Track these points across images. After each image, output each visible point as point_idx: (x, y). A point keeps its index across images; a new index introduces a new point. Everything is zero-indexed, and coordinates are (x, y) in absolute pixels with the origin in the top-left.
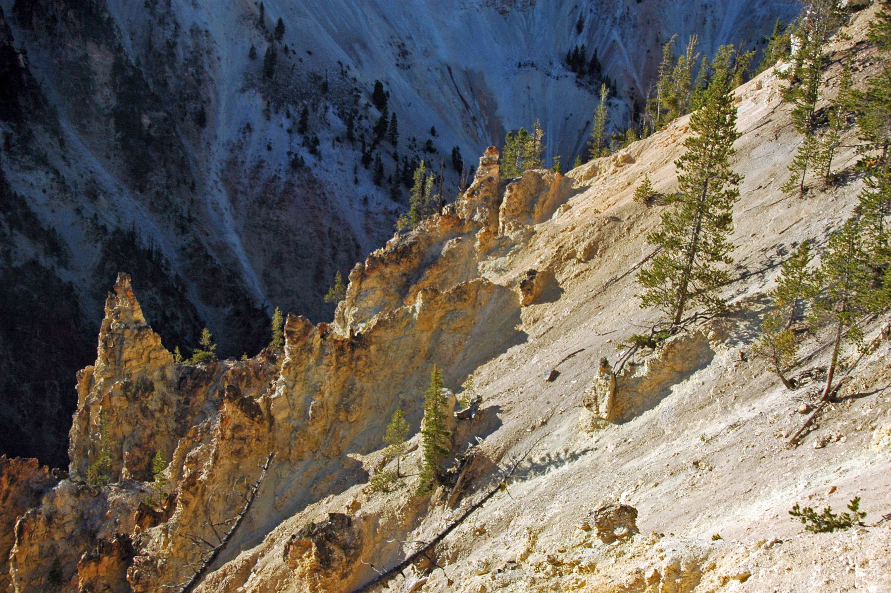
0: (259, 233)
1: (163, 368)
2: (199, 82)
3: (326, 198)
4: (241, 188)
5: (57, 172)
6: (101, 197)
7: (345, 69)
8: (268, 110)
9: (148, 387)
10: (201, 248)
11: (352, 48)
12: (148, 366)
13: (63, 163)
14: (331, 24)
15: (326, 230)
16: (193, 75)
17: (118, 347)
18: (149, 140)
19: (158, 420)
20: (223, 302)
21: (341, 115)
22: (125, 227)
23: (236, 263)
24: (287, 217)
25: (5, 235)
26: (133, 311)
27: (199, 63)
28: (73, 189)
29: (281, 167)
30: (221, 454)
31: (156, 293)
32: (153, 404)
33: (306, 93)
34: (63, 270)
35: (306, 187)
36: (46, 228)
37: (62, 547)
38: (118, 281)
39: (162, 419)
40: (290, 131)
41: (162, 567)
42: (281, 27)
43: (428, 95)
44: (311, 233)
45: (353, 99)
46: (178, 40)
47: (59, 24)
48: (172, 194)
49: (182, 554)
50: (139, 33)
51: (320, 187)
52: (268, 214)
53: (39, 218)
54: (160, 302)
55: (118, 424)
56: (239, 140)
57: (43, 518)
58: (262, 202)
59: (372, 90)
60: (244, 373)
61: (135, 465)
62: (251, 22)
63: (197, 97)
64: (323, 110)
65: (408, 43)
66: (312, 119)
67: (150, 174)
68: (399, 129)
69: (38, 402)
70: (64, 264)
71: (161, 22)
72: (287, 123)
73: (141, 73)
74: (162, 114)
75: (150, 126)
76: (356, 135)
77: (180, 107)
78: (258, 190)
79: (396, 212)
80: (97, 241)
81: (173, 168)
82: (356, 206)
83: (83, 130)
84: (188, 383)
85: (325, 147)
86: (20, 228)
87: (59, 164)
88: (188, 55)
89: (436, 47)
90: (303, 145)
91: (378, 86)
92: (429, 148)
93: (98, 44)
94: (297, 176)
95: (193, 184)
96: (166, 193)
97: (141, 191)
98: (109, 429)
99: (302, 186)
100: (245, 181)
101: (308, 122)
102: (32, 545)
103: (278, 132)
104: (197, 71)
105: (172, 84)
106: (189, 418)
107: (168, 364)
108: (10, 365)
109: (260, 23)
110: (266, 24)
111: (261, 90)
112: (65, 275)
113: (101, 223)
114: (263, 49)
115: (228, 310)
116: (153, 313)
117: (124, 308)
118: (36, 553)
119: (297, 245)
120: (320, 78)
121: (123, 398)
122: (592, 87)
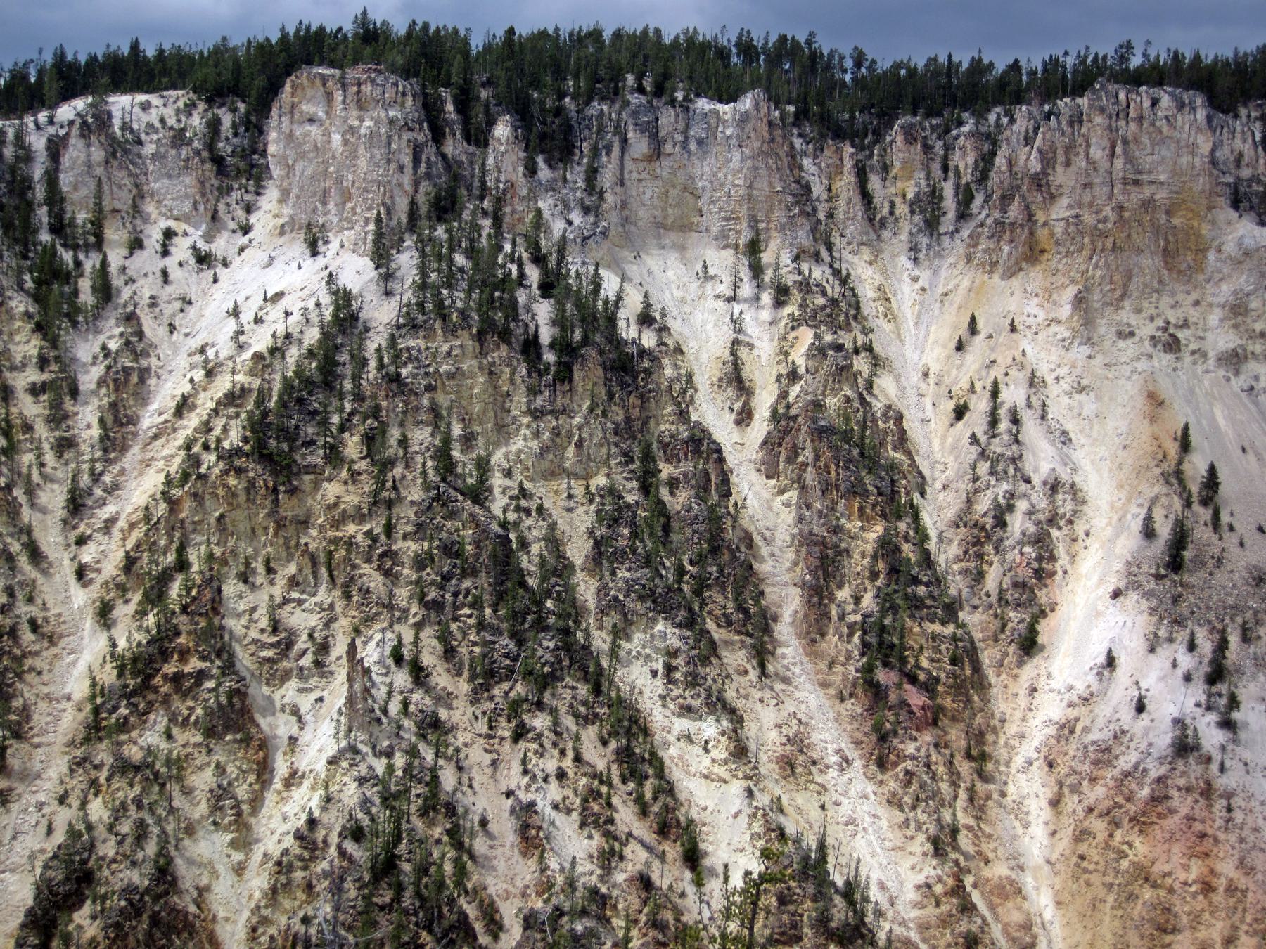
15: (1221, 884)
42: (1212, 482)
99: (1188, 790)
104: (1040, 559)
109: (1176, 476)
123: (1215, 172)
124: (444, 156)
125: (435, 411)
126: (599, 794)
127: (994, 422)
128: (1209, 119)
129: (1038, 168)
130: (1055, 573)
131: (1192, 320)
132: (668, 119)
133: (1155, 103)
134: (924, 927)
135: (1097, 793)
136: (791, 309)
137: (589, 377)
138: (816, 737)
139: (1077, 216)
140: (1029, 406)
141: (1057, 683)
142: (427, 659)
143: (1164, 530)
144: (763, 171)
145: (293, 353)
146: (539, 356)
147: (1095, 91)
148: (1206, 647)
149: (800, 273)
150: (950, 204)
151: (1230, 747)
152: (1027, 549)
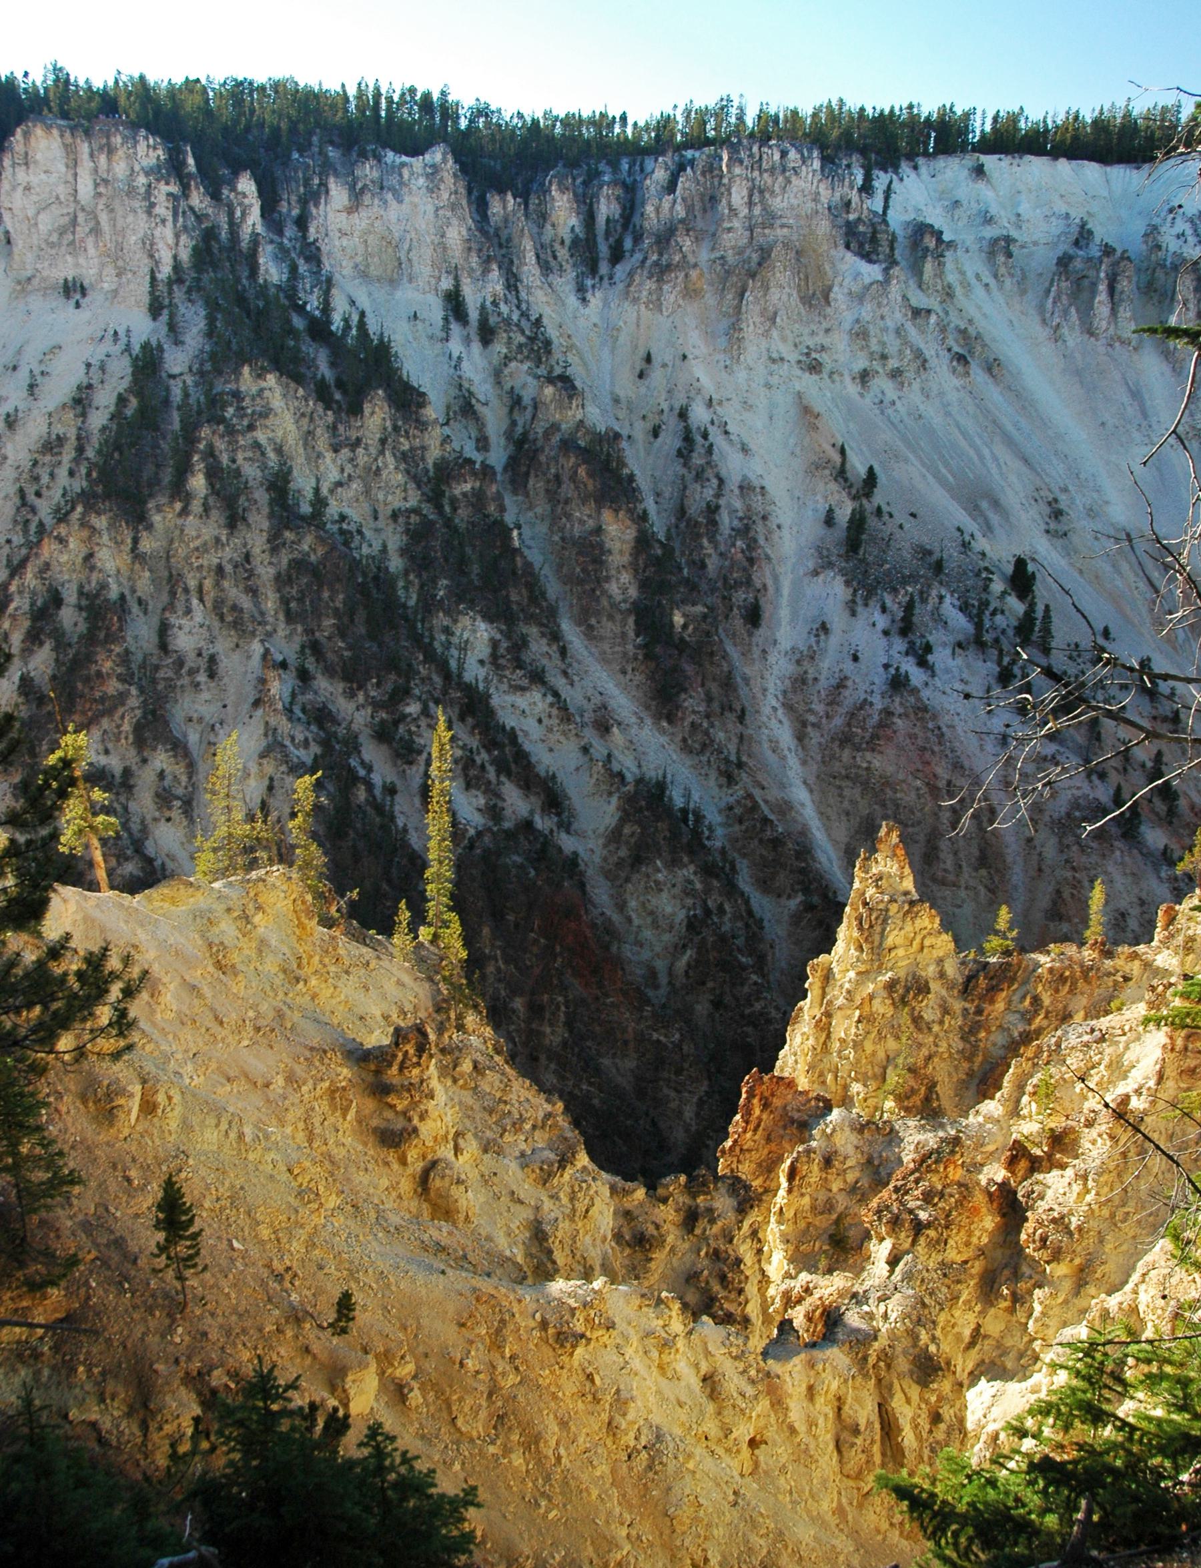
0: (840, 787)
1: (940, 961)
2: (751, 561)
3: (943, 735)
4: (812, 719)
5: (556, 694)
6: (615, 730)
7: (967, 538)
8: (853, 601)
9: (923, 989)
10: (755, 807)
11: (977, 507)
12: (920, 957)
13: (564, 681)
14: (944, 471)
15: (942, 784)
16: (743, 551)
17: (878, 929)
18: (681, 646)
19: (937, 1036)
20: (788, 891)
21: (964, 608)
22: (652, 773)
23: (804, 832)
24: (881, 763)
25: (489, 782)
26: (901, 878)
27: (752, 534)
28: (578, 719)
29: (875, 688)
30: (1168, 1072)
31: (695, 873)
32: (929, 1009)
33: (910, 576)
34: (563, 835)
35: (912, 716)
36: (543, 774)
37: (842, 1202)
38: (883, 832)
39: (942, 1034)
40: (886, 633)
41: (1080, 1229)
42: (871, 479)
43: (1097, 577)
44: (918, 789)
45: (981, 583)
46: (722, 502)
47: (564, 486)
48: (713, 726)
49: (1106, 1212)
50: (667, 495)
51: (934, 717)
53: (533, 759)
54: (698, 886)
55: (881, 1038)
56: (810, 647)
57: (818, 1158)
58: (845, 739)
59: (1009, 569)
60: (1067, 973)
61: (908, 1098)
62: (827, 472)
63: (749, 582)
65: (1062, 497)
66: (921, 614)
67: (683, 696)
68: (1053, 628)
69: (534, 1026)
70: (566, 826)
71: (699, 476)
72: (882, 622)
73: (673, 549)
74: (700, 609)
75: (685, 626)
76: (987, 638)
77: (724, 598)
78: (838, 721)
79: (1053, 757)
80: (610, 794)
81: (714, 688)
82: (990, 748)
83: (590, 633)
84: (980, 983)
85: (940, 657)
86: (509, 775)
87: (560, 683)
88: (736, 523)
89: (1107, 503)
90: (907, 654)
91: (1020, 563)
93: (616, 511)
94: (898, 700)
95: (743, 711)
96: (705, 725)
97: (670, 722)
98: (869, 1047)
99: (907, 716)
100: (819, 708)
101: (915, 619)
102: (802, 1195)
103: (867, 638)
104: (748, 546)
105: (712, 564)
106: (983, 1034)
107: (947, 955)
108: (499, 970)
109: (841, 474)
110: (849, 475)
112: (568, 843)
113: (616, 767)
114: (844, 512)
115: (794, 903)
116: (689, 902)
117: (886, 871)
118: (807, 1207)
119: (897, 806)
120: (930, 553)
121: (888, 1002)
124: (191, 208)
125: (257, 445)
126: (474, 761)
127: (688, 438)
129: (682, 214)
132: (368, 171)
134: (734, 840)
136: (499, 348)
137: (377, 415)
138: (613, 704)
139: (722, 257)
141: (785, 643)
142: (310, 664)
144: (455, 222)
145: (105, 399)
146: (331, 395)
149: (499, 314)
150: (604, 249)
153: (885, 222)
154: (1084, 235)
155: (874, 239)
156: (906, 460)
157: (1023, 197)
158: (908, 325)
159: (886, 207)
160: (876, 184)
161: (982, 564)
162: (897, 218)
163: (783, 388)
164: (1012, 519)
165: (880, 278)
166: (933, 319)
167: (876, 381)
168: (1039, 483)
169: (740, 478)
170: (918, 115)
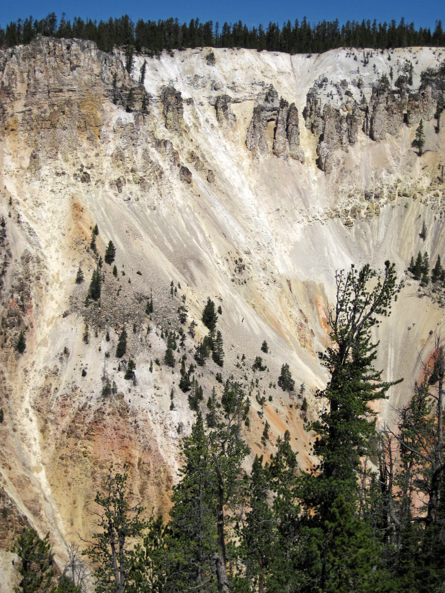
3: (138, 426)
4: (51, 416)
11: (185, 266)
15: (135, 461)
29: (94, 395)
51: (134, 414)
52: (76, 444)
58: (70, 432)
64: (146, 331)
72: (106, 347)
76: (177, 356)
78: (67, 419)
85: (141, 372)
90: (119, 369)
92: (258, 365)
99: (113, 414)
101: (129, 345)
104: (22, 299)
111: (84, 313)
122: (434, 295)
123: (102, 83)
128: (98, 55)
130: (31, 307)
131: (94, 164)
133: (68, 48)
135: (65, 423)
139: (30, 110)
140: (10, 216)
143: (88, 279)
147: (36, 41)
148: (115, 337)
151: (133, 388)
152: (16, 295)
153: (142, 88)
154: (270, 94)
155: (130, 98)
156: (140, 236)
157: (237, 72)
158: (153, 150)
159: (143, 77)
160: (135, 65)
161: (182, 304)
162: (152, 87)
163: (63, 191)
164: (209, 275)
165: (133, 121)
166: (168, 147)
167: (128, 185)
168: (230, 248)
169: (23, 251)
170: (177, 25)
